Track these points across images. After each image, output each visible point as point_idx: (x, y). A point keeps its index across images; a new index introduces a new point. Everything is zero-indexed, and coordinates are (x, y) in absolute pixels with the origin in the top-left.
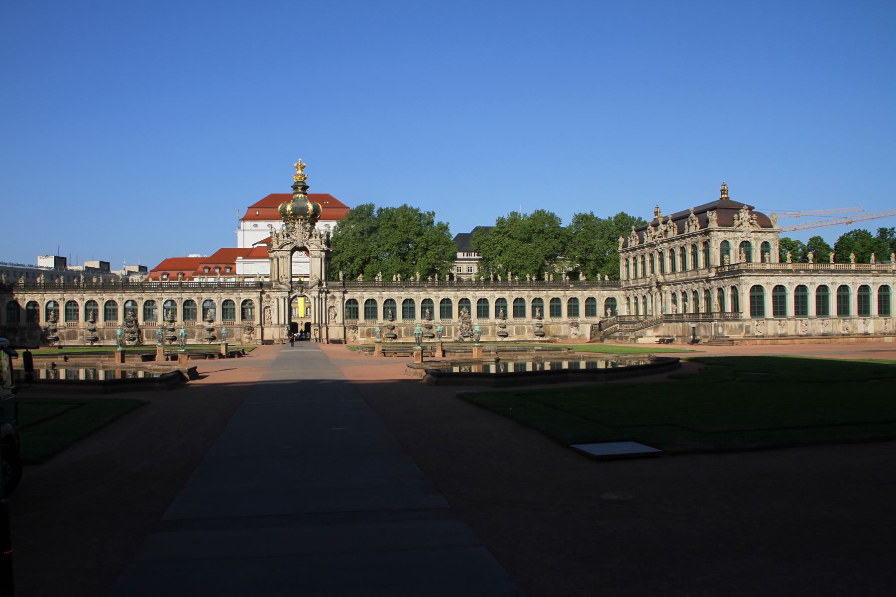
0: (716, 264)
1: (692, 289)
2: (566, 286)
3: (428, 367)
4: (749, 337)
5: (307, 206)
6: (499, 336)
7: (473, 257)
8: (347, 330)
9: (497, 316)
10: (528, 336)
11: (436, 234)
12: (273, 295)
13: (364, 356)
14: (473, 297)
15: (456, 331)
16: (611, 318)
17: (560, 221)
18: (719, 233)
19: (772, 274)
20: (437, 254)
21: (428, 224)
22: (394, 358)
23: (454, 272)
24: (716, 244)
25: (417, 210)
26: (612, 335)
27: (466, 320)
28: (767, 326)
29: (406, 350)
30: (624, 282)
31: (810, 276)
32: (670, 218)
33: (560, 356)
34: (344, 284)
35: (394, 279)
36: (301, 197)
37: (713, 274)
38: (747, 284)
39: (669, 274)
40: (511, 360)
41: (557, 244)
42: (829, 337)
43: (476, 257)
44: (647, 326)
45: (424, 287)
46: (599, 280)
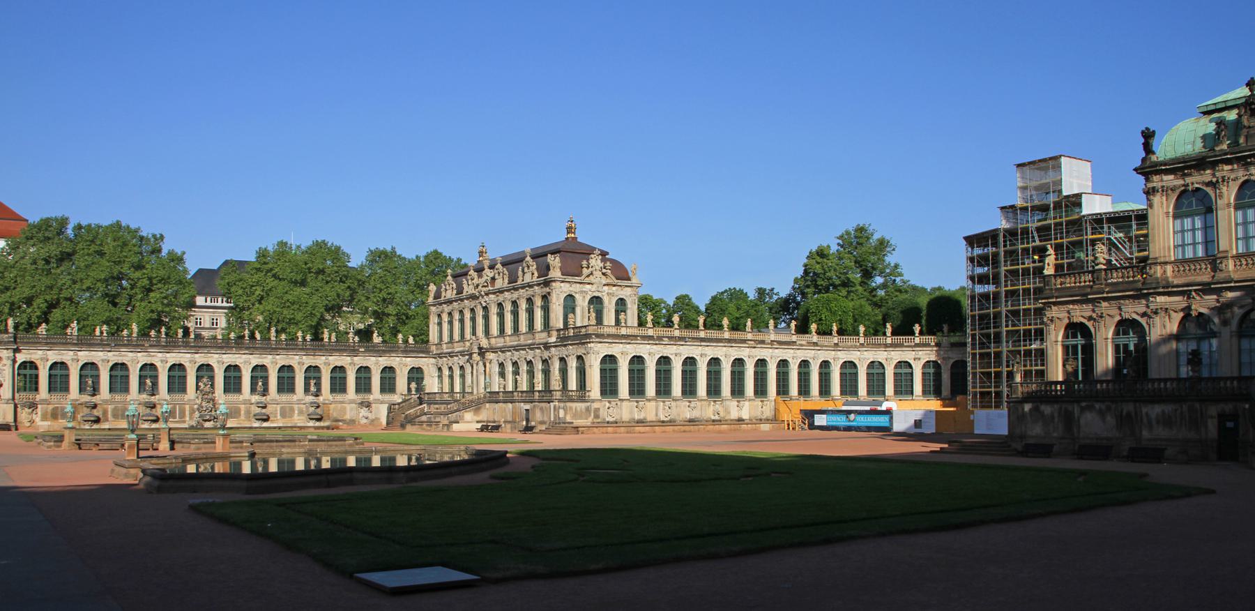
0: (557, 326)
1: (525, 359)
2: (354, 350)
3: (147, 465)
4: (599, 423)
6: (257, 419)
7: (219, 304)
8: (19, 410)
10: (299, 420)
11: (164, 268)
13: (47, 448)
14: (218, 362)
15: (192, 412)
17: (349, 258)
18: (562, 285)
19: (629, 341)
20: (165, 298)
21: (153, 252)
22: (95, 451)
23: (191, 324)
25: (137, 231)
26: (417, 420)
27: (207, 395)
28: (621, 409)
29: (114, 441)
31: (675, 345)
32: (499, 261)
33: (343, 449)
34: (15, 338)
35: (98, 333)
37: (553, 339)
38: (596, 353)
39: (495, 337)
40: (273, 455)
41: (343, 290)
42: (697, 423)
43: (225, 304)
44: (466, 407)
45: (143, 345)
46: (400, 342)
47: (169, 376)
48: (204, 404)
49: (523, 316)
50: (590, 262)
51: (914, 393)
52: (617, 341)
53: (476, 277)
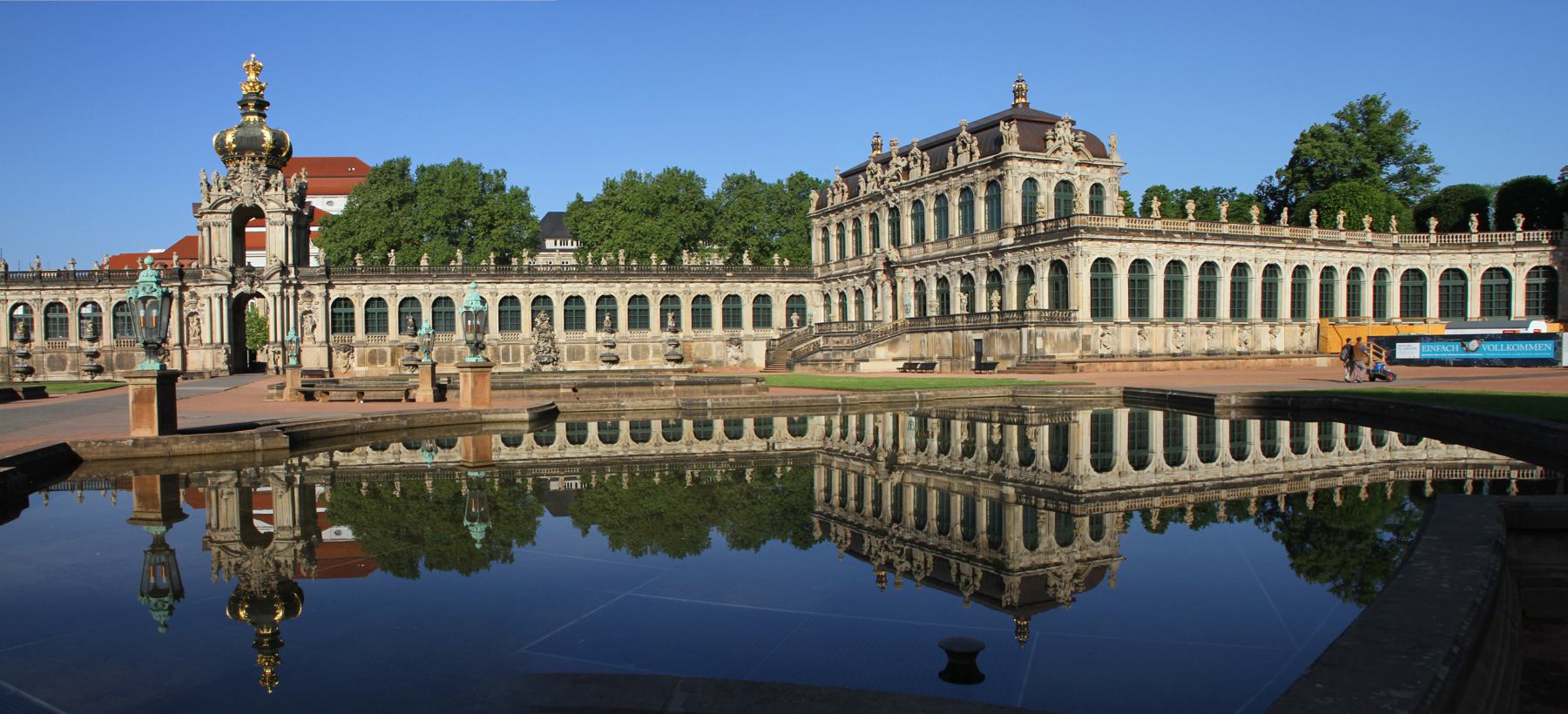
2: (720, 275)
4: (1089, 356)
7: (569, 247)
9: (599, 326)
10: (654, 362)
18: (1021, 163)
24: (1015, 184)
37: (1009, 241)
38: (1087, 252)
39: (909, 247)
43: (575, 246)
46: (776, 264)
49: (955, 215)
51: (1513, 313)
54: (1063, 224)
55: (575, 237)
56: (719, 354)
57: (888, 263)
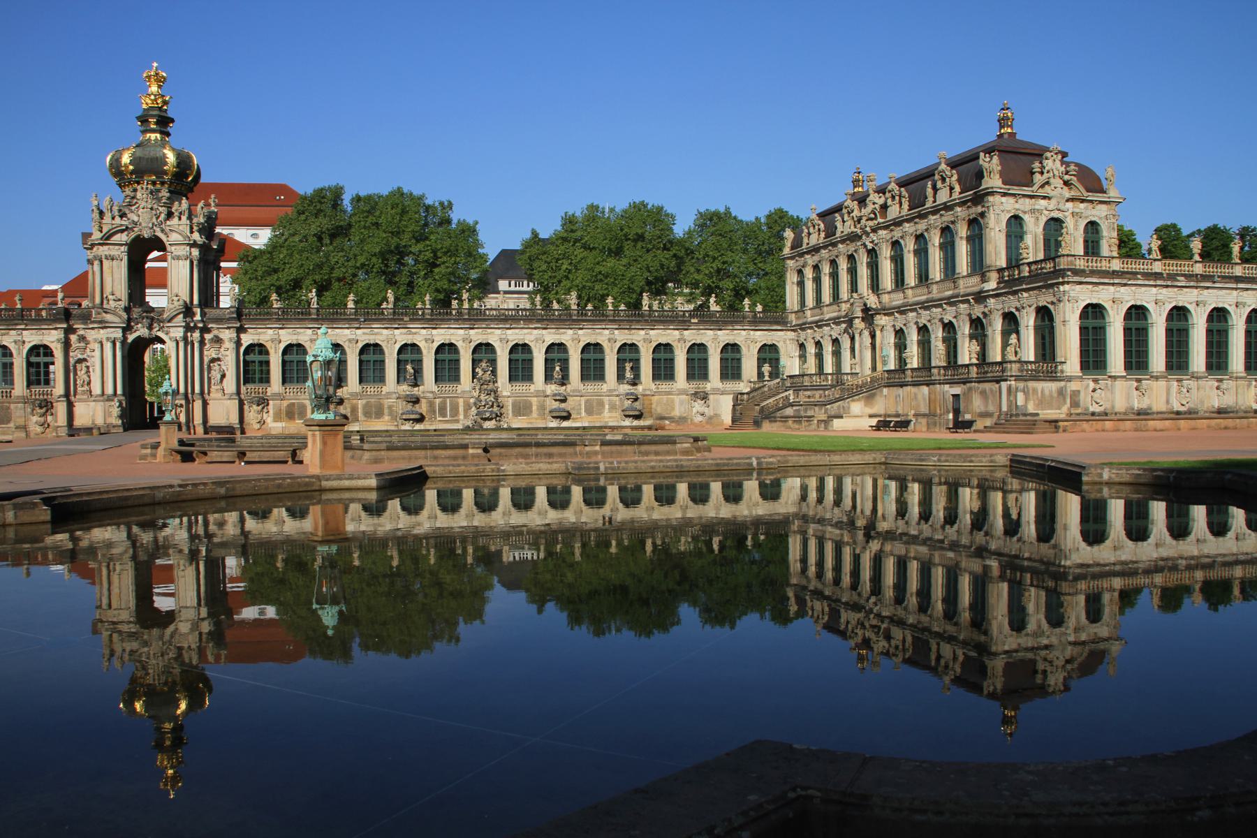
0: (998, 264)
1: (941, 320)
2: (685, 322)
5: (164, 154)
6: (553, 417)
7: (525, 288)
8: (246, 407)
9: (548, 377)
10: (610, 417)
12: (92, 335)
14: (501, 340)
15: (467, 407)
16: (769, 383)
18: (1004, 199)
19: (1125, 281)
21: (440, 224)
24: (998, 221)
25: (421, 198)
26: (778, 414)
27: (487, 385)
30: (794, 315)
31: (1196, 287)
36: (156, 139)
37: (992, 285)
39: (889, 293)
41: (667, 259)
42: (1231, 415)
46: (747, 309)
47: (436, 361)
48: (483, 397)
49: (935, 256)
50: (1045, 164)
52: (1106, 281)
53: (856, 207)
54: (1049, 266)
55: (530, 278)
56: (683, 410)
57: (866, 309)
